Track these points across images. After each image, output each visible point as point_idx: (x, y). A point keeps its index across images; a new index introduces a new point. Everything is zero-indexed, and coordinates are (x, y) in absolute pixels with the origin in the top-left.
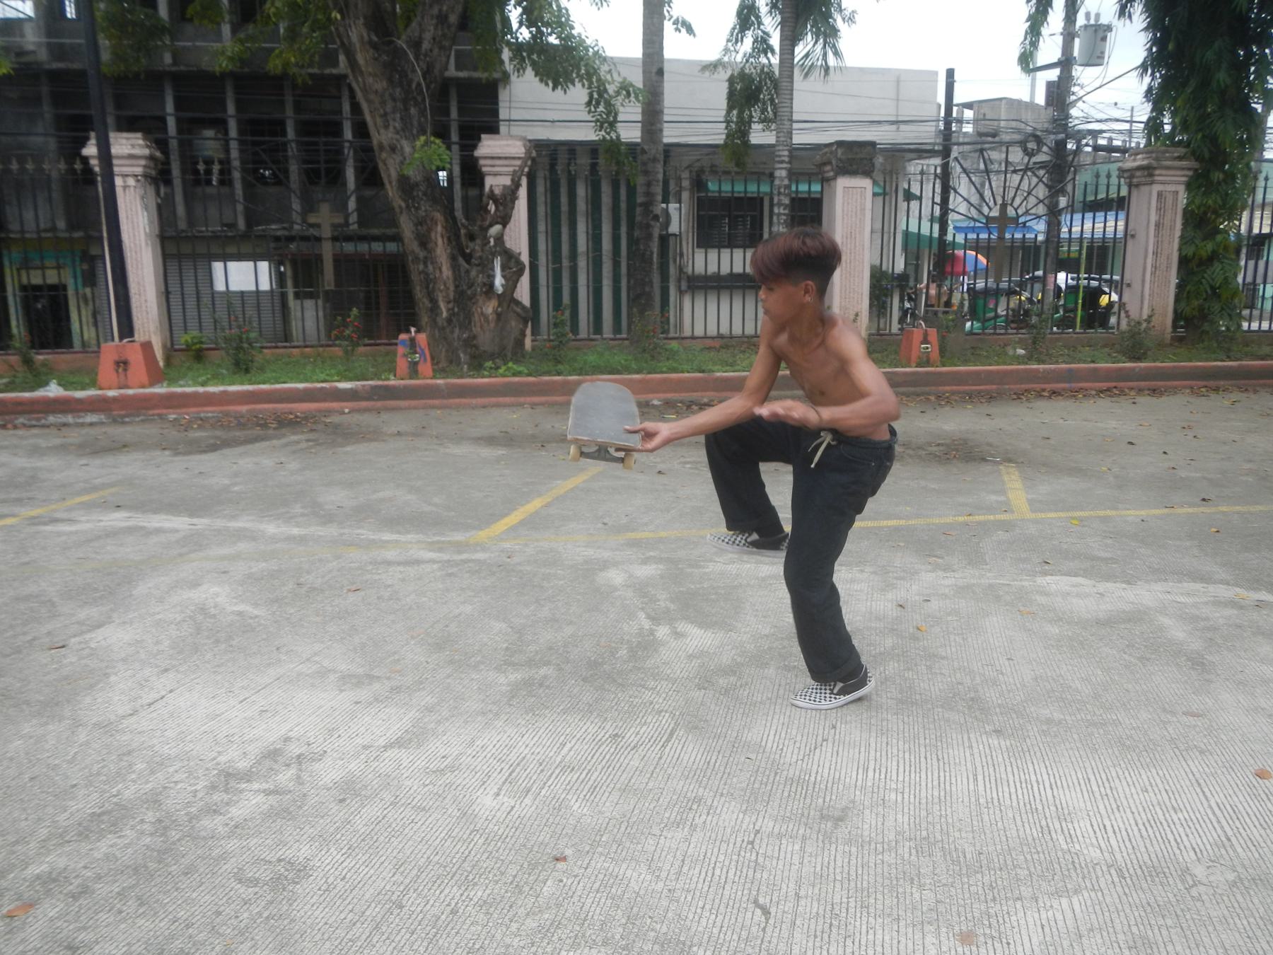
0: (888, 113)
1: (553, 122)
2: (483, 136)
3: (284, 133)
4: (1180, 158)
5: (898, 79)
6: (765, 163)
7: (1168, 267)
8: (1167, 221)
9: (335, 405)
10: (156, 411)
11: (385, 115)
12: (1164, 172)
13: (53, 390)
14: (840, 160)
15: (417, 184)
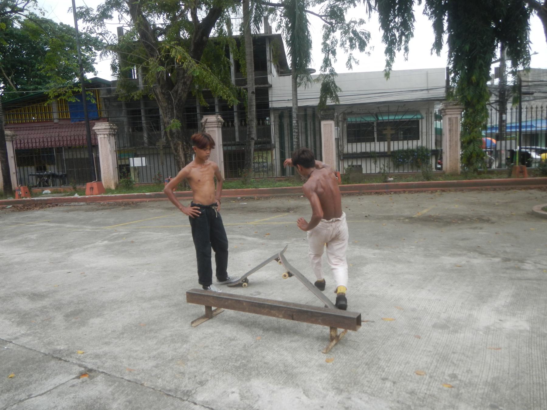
0: (424, 86)
1: (289, 100)
2: (204, 116)
3: (196, 112)
4: (456, 105)
5: (427, 73)
6: (373, 109)
7: (457, 145)
8: (454, 128)
9: (145, 199)
10: (98, 202)
11: (166, 113)
12: (449, 110)
13: (76, 196)
14: (322, 115)
15: (174, 133)
